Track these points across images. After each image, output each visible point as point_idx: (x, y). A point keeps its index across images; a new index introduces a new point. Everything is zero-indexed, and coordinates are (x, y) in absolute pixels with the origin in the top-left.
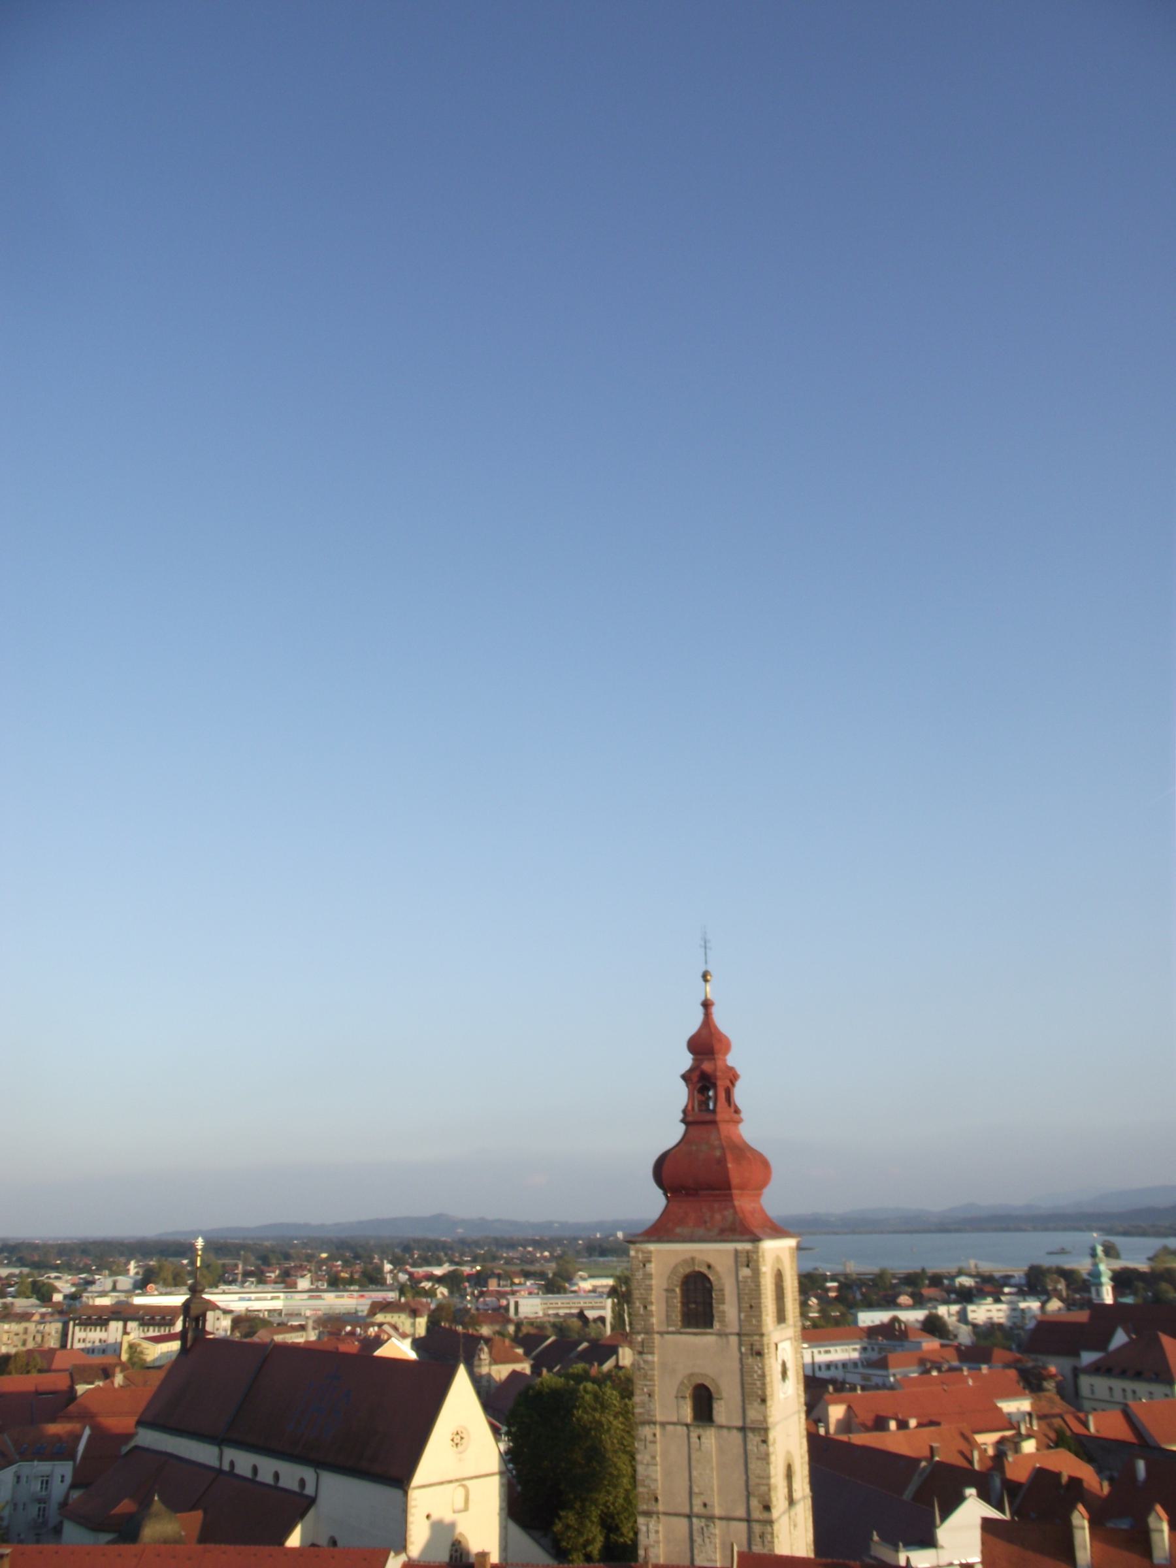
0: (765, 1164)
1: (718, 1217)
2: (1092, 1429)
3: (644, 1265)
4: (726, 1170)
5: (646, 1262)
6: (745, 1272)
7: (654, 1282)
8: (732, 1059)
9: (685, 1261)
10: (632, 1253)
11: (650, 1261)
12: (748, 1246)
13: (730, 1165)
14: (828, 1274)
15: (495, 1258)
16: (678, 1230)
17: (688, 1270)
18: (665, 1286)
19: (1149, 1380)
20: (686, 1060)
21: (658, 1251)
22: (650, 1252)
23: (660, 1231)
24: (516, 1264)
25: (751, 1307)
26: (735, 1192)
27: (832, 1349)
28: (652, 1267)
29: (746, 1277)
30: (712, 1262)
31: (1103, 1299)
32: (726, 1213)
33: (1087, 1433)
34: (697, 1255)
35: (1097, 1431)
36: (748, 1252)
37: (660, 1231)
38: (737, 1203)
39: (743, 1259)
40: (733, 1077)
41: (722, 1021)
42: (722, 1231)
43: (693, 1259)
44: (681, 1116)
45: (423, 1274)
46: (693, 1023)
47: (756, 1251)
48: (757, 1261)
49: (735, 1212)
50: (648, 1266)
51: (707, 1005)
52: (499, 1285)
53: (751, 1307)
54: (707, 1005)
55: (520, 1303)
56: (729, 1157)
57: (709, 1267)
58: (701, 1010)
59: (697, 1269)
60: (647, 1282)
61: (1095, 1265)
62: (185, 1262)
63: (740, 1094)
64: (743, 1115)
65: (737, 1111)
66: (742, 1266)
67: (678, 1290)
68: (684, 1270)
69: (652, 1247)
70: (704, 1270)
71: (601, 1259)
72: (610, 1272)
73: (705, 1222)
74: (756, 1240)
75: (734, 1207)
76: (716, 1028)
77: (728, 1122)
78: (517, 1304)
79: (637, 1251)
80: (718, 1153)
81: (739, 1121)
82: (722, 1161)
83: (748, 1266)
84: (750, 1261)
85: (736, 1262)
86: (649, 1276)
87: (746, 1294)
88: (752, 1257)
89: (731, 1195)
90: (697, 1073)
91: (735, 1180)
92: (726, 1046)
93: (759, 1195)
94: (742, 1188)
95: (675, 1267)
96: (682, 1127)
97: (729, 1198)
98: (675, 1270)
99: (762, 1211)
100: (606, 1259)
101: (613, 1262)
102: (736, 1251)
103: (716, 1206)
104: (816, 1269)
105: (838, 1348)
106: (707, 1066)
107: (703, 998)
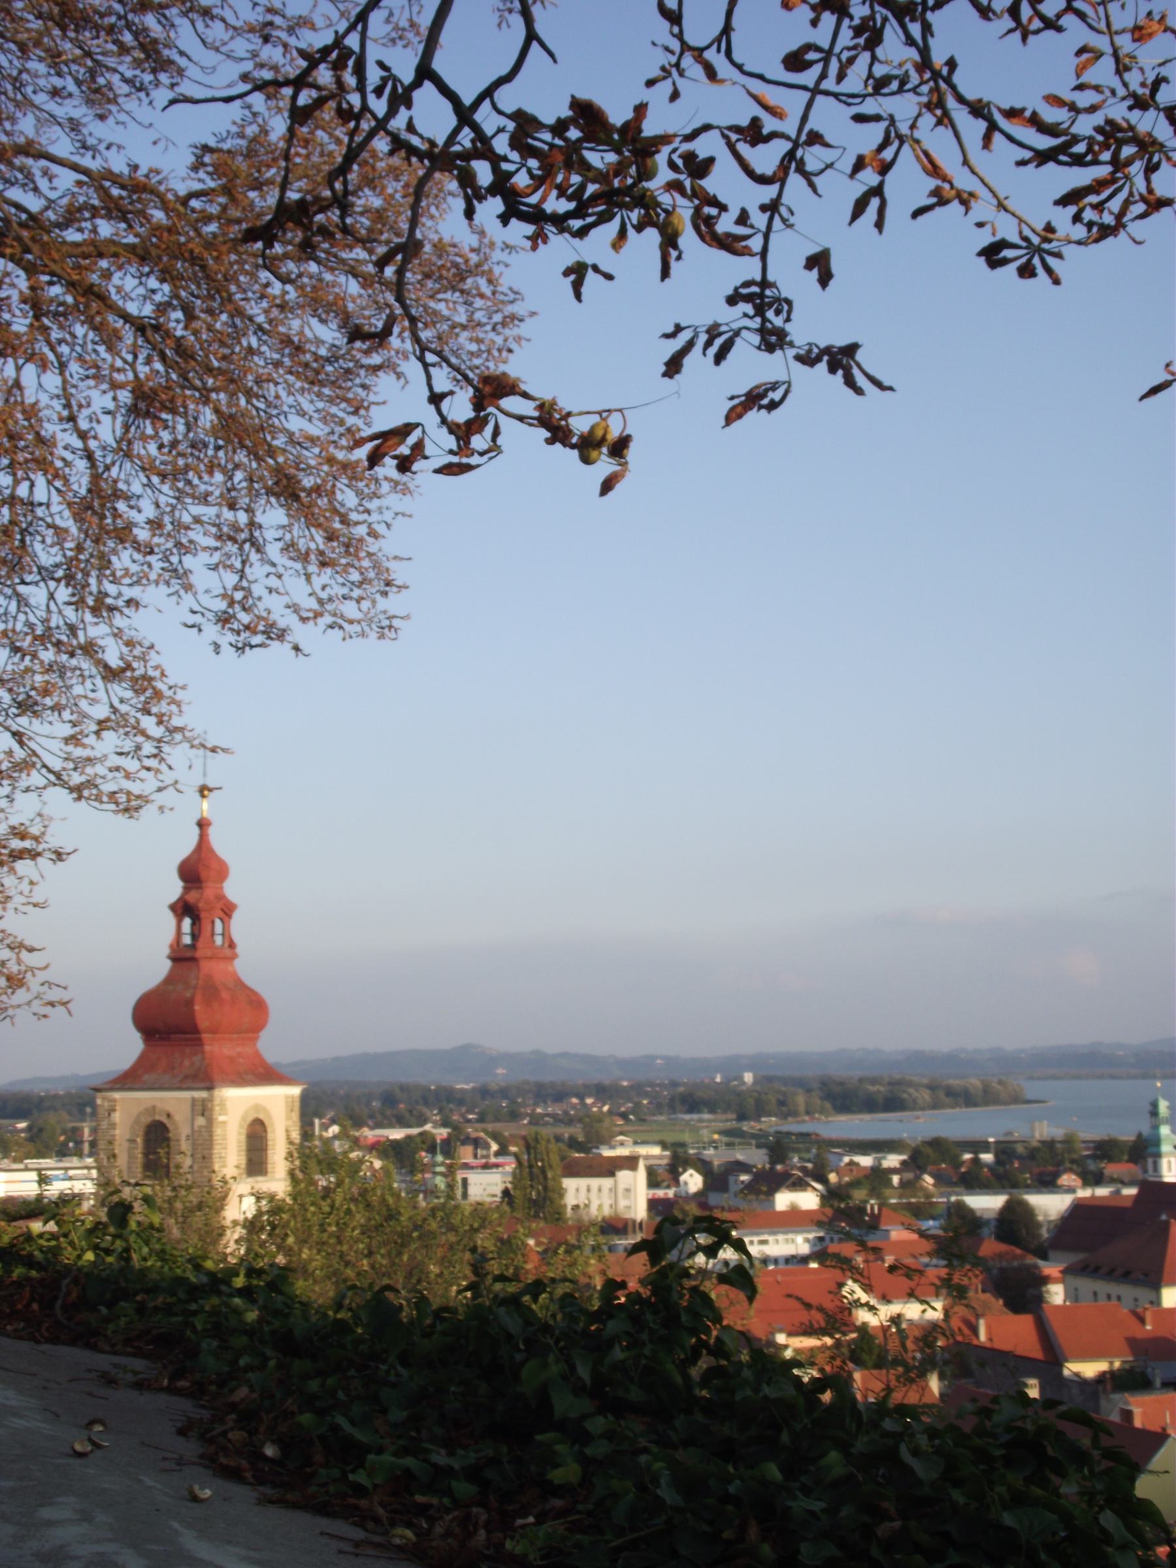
0: (257, 1005)
1: (187, 1063)
2: (983, 1337)
4: (192, 1012)
5: (112, 1110)
6: (201, 1121)
7: (117, 1132)
8: (232, 889)
9: (147, 1109)
10: (99, 1101)
11: (114, 1110)
12: (204, 1094)
13: (197, 1007)
14: (991, 1140)
15: (514, 1116)
16: (146, 1077)
17: (149, 1120)
18: (128, 1137)
19: (1136, 1283)
20: (175, 889)
21: (123, 1099)
22: (114, 1100)
23: (128, 1080)
24: (546, 1124)
25: (204, 1157)
26: (205, 1036)
27: (771, 1238)
28: (117, 1117)
29: (201, 1127)
31: (1161, 1176)
33: (975, 1342)
34: (158, 1104)
35: (990, 1339)
36: (203, 1100)
37: (128, 1080)
38: (207, 1048)
40: (228, 910)
41: (218, 841)
42: (186, 1077)
43: (154, 1107)
44: (167, 951)
45: (375, 1139)
46: (186, 846)
47: (211, 1099)
48: (212, 1110)
50: (113, 1115)
51: (203, 824)
52: (475, 1156)
53: (204, 1157)
54: (203, 824)
55: (470, 1181)
56: (199, 997)
57: (169, 1115)
58: (197, 830)
59: (157, 1118)
60: (112, 1132)
61: (1156, 1127)
62: (22, 1125)
63: (239, 926)
64: (238, 950)
65: (232, 945)
67: (139, 1140)
68: (146, 1120)
69: (117, 1095)
70: (164, 1119)
71: (687, 1117)
72: (657, 1137)
73: (173, 1068)
74: (210, 1088)
75: (203, 1052)
76: (212, 851)
77: (210, 958)
78: (465, 1181)
79: (104, 1099)
80: (188, 994)
81: (235, 956)
82: (190, 1003)
83: (203, 1115)
84: (204, 1109)
85: (193, 1110)
86: (113, 1126)
89: (200, 1039)
90: (181, 904)
91: (203, 1021)
92: (222, 871)
93: (256, 1039)
94: (214, 1031)
95: (139, 1115)
96: (167, 964)
97: (199, 1042)
98: (137, 1121)
99: (257, 1055)
100: (695, 1116)
101: (701, 1121)
102: (194, 1100)
103: (188, 1050)
104: (1010, 1133)
105: (781, 1237)
106: (192, 897)
107: (199, 817)
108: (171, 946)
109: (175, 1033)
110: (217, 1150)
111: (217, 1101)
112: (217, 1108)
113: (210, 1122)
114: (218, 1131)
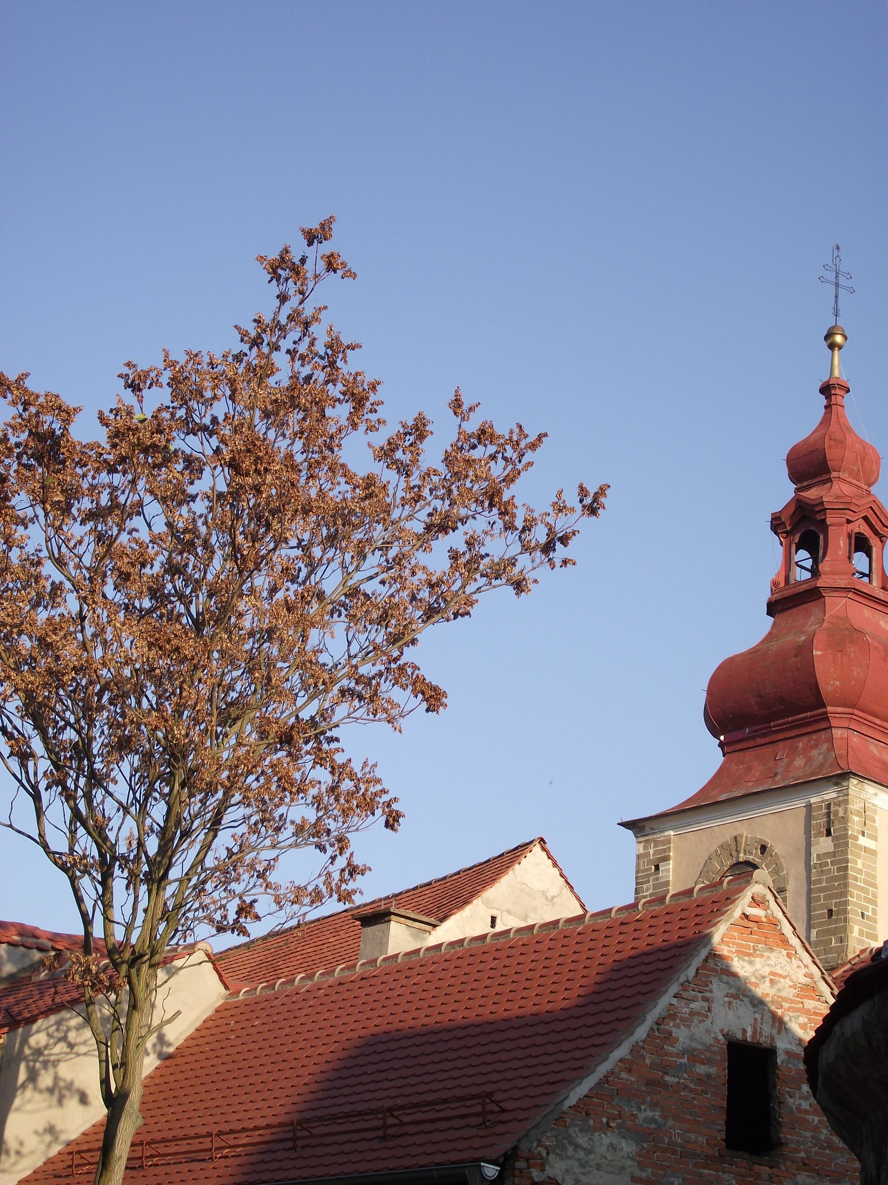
1: (799, 762)
3: (657, 868)
4: (810, 664)
6: (824, 844)
11: (666, 859)
25: (830, 912)
30: (770, 842)
32: (815, 753)
38: (837, 733)
39: (820, 821)
48: (845, 820)
49: (832, 748)
57: (763, 848)
66: (819, 835)
75: (831, 739)
76: (846, 429)
83: (828, 833)
87: (822, 890)
88: (837, 812)
89: (825, 718)
97: (822, 723)
108: (775, 584)
109: (778, 715)
110: (855, 899)
111: (855, 805)
112: (855, 820)
113: (842, 843)
114: (857, 864)
